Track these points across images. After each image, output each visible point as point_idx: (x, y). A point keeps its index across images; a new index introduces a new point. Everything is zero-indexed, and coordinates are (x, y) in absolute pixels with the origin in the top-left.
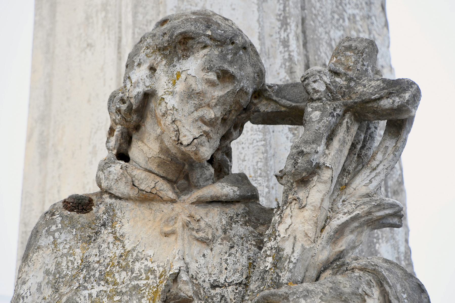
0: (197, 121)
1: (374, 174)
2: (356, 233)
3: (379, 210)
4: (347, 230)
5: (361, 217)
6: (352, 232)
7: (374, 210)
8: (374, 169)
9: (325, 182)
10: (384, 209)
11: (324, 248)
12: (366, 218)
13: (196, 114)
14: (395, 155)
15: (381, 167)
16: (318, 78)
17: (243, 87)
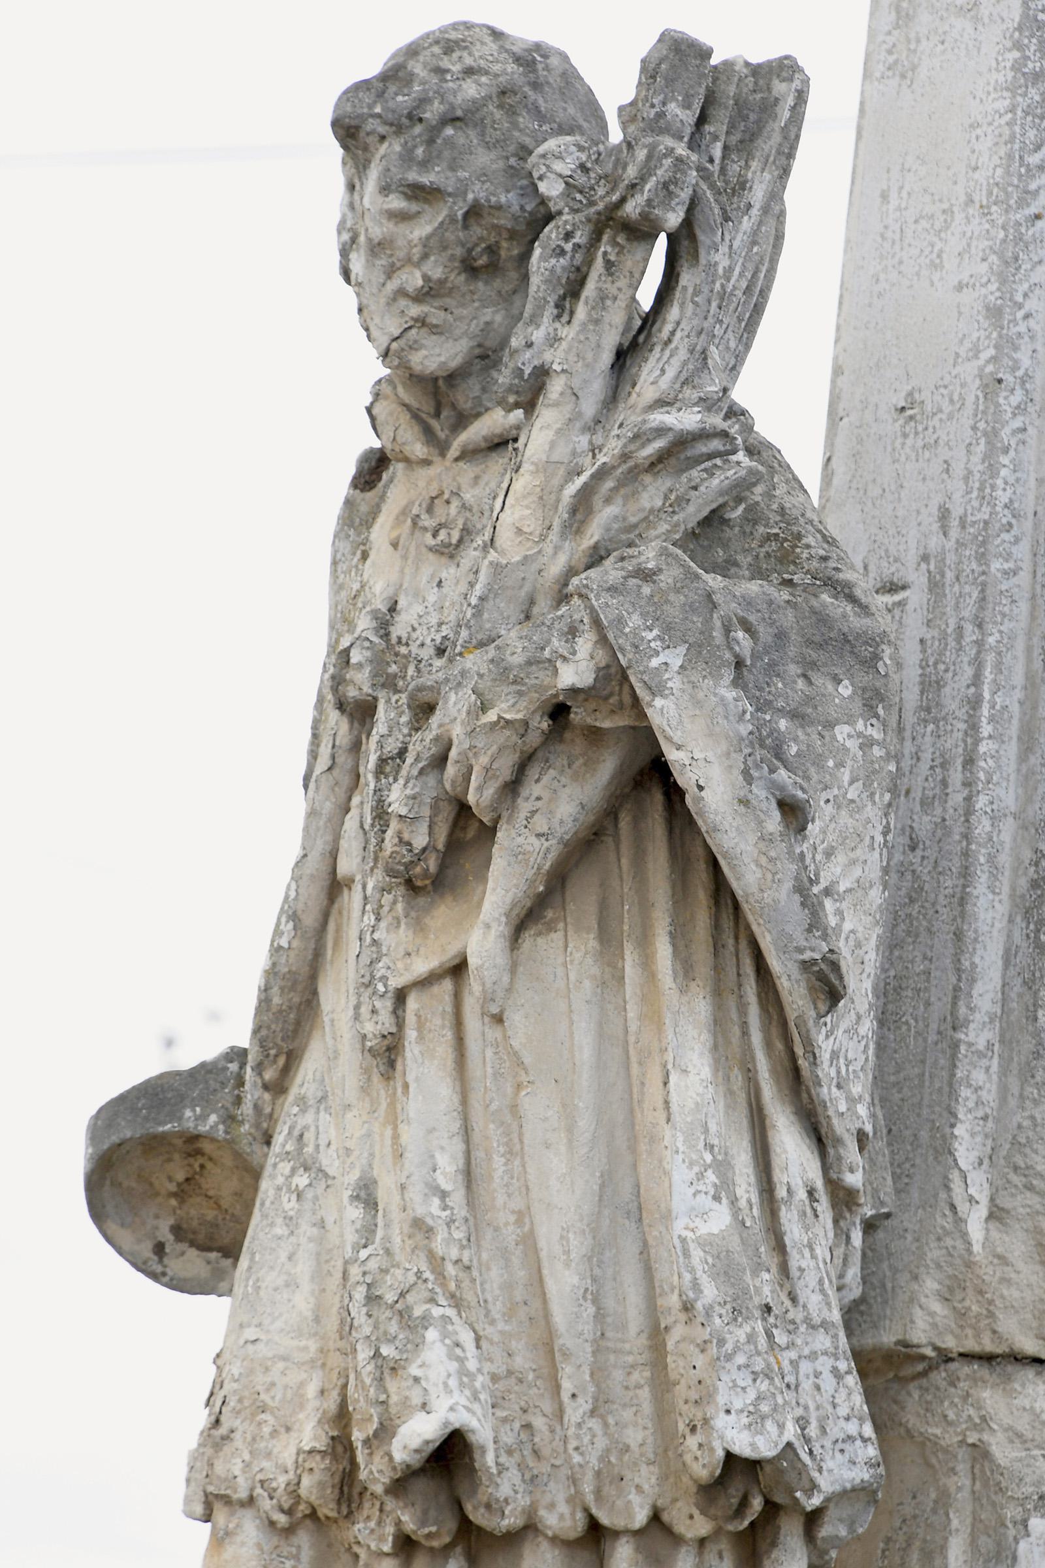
0: (394, 299)
1: (667, 353)
2: (619, 501)
3: (643, 446)
4: (597, 501)
5: (614, 468)
6: (608, 501)
7: (632, 447)
8: (669, 341)
9: (556, 404)
10: (649, 441)
11: (557, 549)
12: (624, 467)
13: (392, 286)
14: (696, 304)
15: (678, 334)
16: (544, 169)
17: (476, 200)
